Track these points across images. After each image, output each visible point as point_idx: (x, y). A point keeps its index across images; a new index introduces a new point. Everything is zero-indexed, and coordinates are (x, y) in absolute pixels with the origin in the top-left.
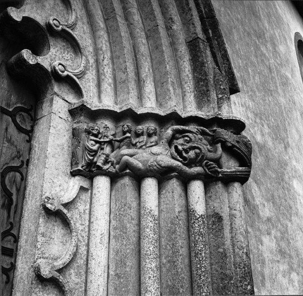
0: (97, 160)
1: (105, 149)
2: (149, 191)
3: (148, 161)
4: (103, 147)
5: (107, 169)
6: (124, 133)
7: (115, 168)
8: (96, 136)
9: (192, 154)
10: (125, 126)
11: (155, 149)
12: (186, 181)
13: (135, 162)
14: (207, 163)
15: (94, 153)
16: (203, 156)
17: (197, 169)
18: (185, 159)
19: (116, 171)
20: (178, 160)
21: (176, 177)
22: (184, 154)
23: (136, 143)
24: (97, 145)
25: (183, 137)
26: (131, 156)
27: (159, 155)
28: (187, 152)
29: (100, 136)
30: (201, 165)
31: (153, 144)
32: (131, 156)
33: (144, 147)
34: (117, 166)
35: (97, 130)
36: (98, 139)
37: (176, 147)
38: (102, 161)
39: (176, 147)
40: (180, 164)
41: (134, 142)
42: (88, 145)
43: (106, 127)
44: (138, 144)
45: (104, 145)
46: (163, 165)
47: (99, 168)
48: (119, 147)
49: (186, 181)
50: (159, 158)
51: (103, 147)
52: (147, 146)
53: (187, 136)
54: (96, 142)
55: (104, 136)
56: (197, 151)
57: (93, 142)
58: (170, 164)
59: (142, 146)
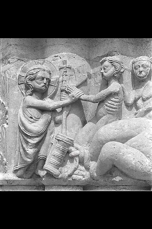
0: (47, 150)
1: (64, 122)
4: (58, 118)
5: (70, 176)
6: (106, 82)
7: (87, 169)
8: (42, 94)
15: (36, 140)
19: (92, 177)
23: (136, 101)
24: (46, 117)
26: (124, 139)
29: (51, 90)
32: (124, 139)
34: (93, 165)
35: (43, 79)
36: (48, 103)
38: (55, 161)
41: (131, 101)
42: (23, 119)
43: (65, 69)
44: (140, 102)
45: (61, 112)
47: (49, 174)
48: (96, 118)
51: (58, 118)
54: (43, 110)
55: (62, 91)
57: (34, 113)
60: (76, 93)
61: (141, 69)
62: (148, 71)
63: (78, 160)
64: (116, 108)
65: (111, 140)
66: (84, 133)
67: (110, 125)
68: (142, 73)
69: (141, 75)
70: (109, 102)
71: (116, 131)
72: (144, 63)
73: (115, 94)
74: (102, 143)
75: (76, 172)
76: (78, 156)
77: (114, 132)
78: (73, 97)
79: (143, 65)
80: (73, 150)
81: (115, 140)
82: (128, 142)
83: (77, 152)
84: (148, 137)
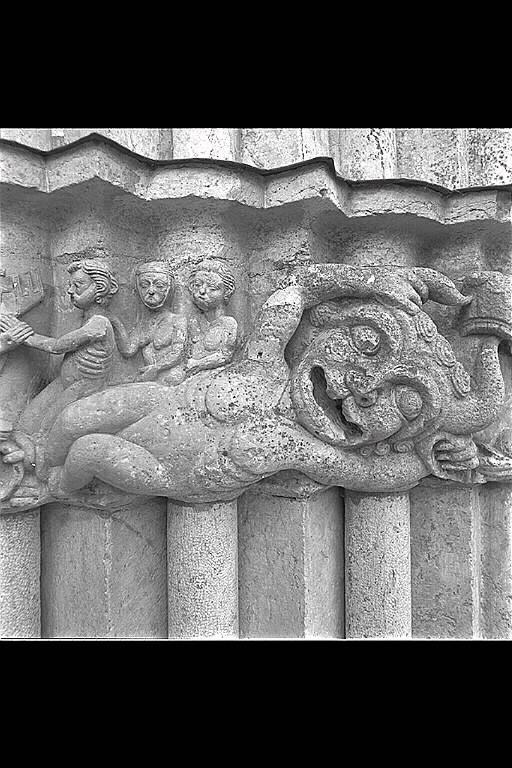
2: (202, 568)
3: (191, 456)
9: (386, 415)
10: (79, 275)
11: (230, 389)
12: (344, 499)
13: (127, 458)
14: (439, 442)
16: (430, 424)
17: (405, 468)
18: (354, 429)
20: (328, 442)
21: (313, 497)
22: (355, 416)
23: (141, 348)
25: (355, 322)
26: (115, 428)
27: (237, 420)
28: (364, 403)
30: (416, 451)
31: (217, 357)
32: (115, 428)
33: (176, 373)
37: (318, 375)
39: (318, 375)
40: (330, 454)
41: (131, 349)
44: (148, 352)
46: (259, 469)
49: (344, 499)
50: (244, 438)
52: (192, 363)
53: (370, 324)
56: (415, 399)
58: (291, 459)
59: (167, 369)
60: (15, 332)
61: (152, 289)
62: (166, 294)
63: (21, 470)
64: (101, 369)
65: (89, 432)
66: (36, 411)
67: (88, 401)
68: (155, 296)
69: (153, 301)
70: (83, 357)
71: (98, 413)
72: (158, 276)
73: (95, 342)
74: (73, 438)
75: (20, 492)
76: (22, 460)
77: (96, 416)
78: (9, 340)
79: (156, 280)
80: (10, 450)
81: (97, 431)
82: (125, 433)
83: (20, 454)
84: (162, 424)
